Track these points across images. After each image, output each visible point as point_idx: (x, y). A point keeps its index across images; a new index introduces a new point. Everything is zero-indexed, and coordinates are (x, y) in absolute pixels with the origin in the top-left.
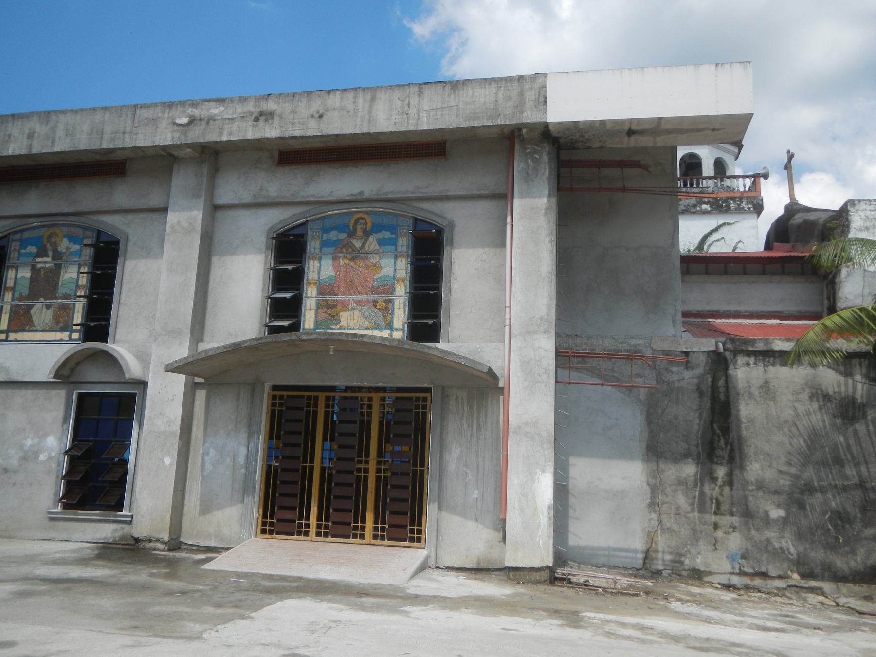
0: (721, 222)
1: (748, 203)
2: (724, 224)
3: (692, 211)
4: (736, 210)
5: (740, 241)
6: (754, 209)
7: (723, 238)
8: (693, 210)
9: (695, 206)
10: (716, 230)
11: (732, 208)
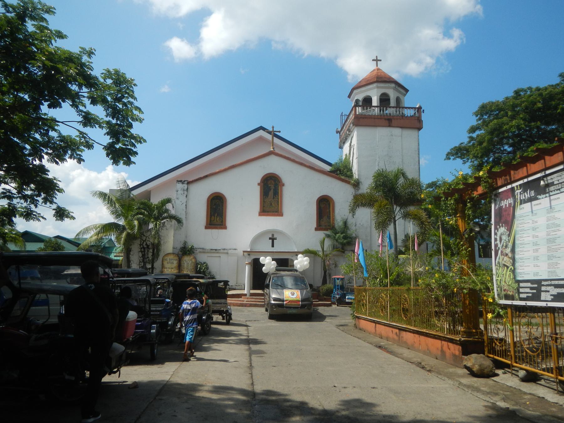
10: (351, 142)
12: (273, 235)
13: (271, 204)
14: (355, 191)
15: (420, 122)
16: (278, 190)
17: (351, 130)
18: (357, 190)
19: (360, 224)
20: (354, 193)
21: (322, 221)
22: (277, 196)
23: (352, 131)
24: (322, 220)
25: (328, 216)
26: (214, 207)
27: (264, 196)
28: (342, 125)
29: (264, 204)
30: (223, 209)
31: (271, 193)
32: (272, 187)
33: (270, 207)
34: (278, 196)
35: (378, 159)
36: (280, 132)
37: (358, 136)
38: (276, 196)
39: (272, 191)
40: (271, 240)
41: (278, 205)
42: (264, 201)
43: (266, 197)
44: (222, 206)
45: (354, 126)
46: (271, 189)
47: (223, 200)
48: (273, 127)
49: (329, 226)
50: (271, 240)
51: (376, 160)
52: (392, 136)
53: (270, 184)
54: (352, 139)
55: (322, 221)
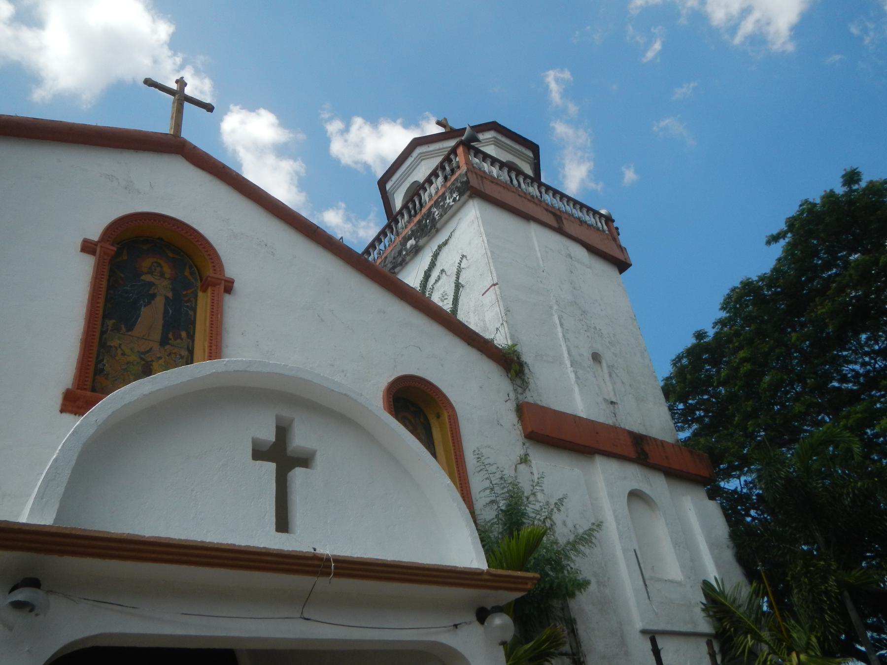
0: (435, 248)
1: (451, 193)
2: (440, 248)
3: (399, 262)
4: (441, 216)
5: (463, 256)
6: (461, 194)
7: (443, 271)
8: (400, 259)
9: (400, 253)
10: (433, 265)
11: (437, 218)
12: (283, 432)
14: (515, 390)
15: (622, 251)
16: (195, 310)
17: (438, 225)
18: (520, 390)
19: (564, 523)
20: (512, 396)
22: (184, 334)
29: (99, 361)
32: (163, 289)
34: (191, 337)
35: (555, 307)
38: (178, 337)
39: (159, 302)
40: (270, 468)
46: (154, 296)
50: (270, 468)
51: (551, 307)
52: (571, 258)
53: (150, 272)
54: (436, 256)
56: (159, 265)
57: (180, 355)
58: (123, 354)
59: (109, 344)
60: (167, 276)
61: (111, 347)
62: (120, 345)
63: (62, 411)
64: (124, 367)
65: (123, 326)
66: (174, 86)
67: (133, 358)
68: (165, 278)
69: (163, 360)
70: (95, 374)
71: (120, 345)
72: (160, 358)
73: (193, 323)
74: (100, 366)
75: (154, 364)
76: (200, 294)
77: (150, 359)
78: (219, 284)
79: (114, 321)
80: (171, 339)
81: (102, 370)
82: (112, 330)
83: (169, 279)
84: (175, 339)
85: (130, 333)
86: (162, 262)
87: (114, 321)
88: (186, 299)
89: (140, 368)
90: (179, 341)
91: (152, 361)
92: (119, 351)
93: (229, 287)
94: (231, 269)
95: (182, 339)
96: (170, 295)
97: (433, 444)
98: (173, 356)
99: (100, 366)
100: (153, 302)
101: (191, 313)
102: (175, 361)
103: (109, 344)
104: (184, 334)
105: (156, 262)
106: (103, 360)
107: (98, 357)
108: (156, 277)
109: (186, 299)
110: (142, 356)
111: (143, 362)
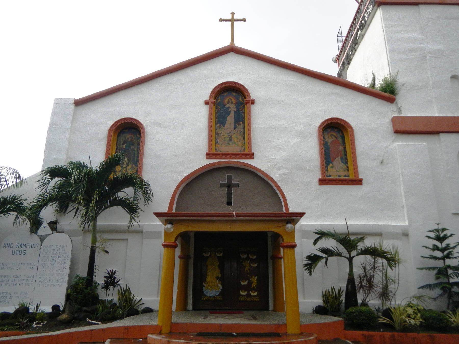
4: (368, 18)
13: (231, 139)
16: (244, 113)
17: (368, 23)
21: (332, 167)
23: (369, 25)
24: (331, 165)
25: (342, 158)
26: (124, 146)
27: (216, 124)
28: (340, 48)
29: (216, 139)
30: (138, 149)
31: (230, 119)
32: (233, 108)
33: (229, 144)
34: (244, 123)
36: (244, 20)
37: (385, 19)
38: (239, 124)
41: (244, 139)
42: (217, 134)
43: (220, 127)
44: (139, 144)
45: (376, 7)
46: (230, 111)
47: (140, 134)
48: (233, 14)
49: (345, 176)
53: (228, 103)
55: (332, 167)
56: (231, 99)
57: (241, 131)
58: (223, 135)
59: (218, 133)
60: (234, 103)
61: (219, 134)
62: (222, 132)
63: (206, 159)
64: (224, 140)
65: (222, 126)
66: (230, 17)
67: (226, 136)
68: (233, 104)
69: (235, 135)
70: (216, 144)
71: (222, 132)
72: (234, 134)
73: (244, 118)
74: (217, 141)
75: (233, 136)
76: (245, 106)
77: (231, 135)
78: (250, 102)
79: (219, 124)
80: (237, 126)
81: (217, 142)
82: (219, 128)
83: (235, 104)
84: (239, 126)
85: (224, 127)
86: (232, 98)
87: (219, 124)
88: (241, 110)
89: (229, 139)
90: (240, 126)
91: (232, 135)
92: (222, 135)
93: (253, 102)
94: (253, 96)
95: (241, 125)
96: (235, 110)
97: (345, 143)
98: (238, 132)
99: (217, 141)
100: (230, 114)
101: (243, 114)
102: (239, 134)
103: (218, 133)
104: (241, 123)
105: (230, 99)
106: (217, 139)
107: (216, 138)
108: (230, 104)
109: (241, 110)
110: (229, 134)
111: (229, 136)
